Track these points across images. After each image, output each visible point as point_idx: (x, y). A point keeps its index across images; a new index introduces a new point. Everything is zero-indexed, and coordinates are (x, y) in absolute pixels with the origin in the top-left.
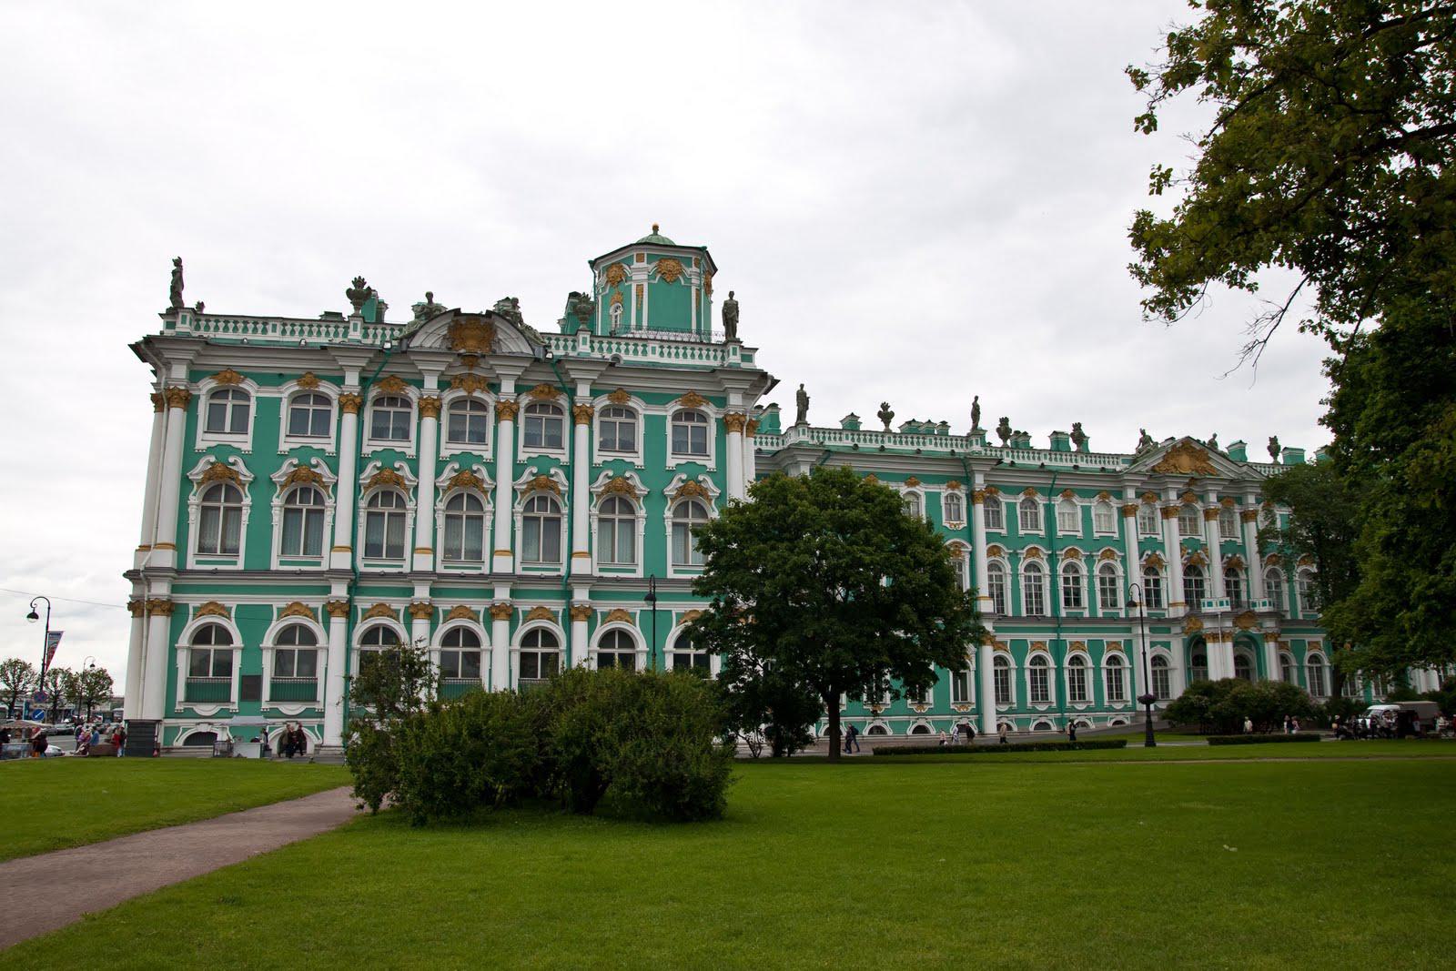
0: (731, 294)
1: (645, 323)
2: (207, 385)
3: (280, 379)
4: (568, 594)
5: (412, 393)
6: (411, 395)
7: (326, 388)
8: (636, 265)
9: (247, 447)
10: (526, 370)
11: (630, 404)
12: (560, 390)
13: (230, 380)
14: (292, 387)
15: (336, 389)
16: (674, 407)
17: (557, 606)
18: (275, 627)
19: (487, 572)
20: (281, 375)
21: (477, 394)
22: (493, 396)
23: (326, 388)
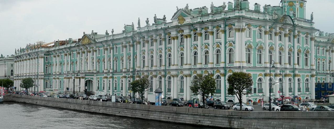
0: (312, 13)
1: (299, 17)
2: (247, 26)
3: (256, 26)
4: (293, 72)
5: (274, 30)
6: (273, 31)
7: (263, 29)
8: (297, 3)
9: (252, 41)
10: (291, 27)
11: (300, 34)
12: (293, 31)
13: (249, 26)
14: (258, 28)
15: (264, 29)
16: (305, 35)
17: (292, 74)
18: (258, 78)
19: (283, 67)
20: (256, 25)
21: (282, 31)
22: (284, 32)
23: (263, 29)
